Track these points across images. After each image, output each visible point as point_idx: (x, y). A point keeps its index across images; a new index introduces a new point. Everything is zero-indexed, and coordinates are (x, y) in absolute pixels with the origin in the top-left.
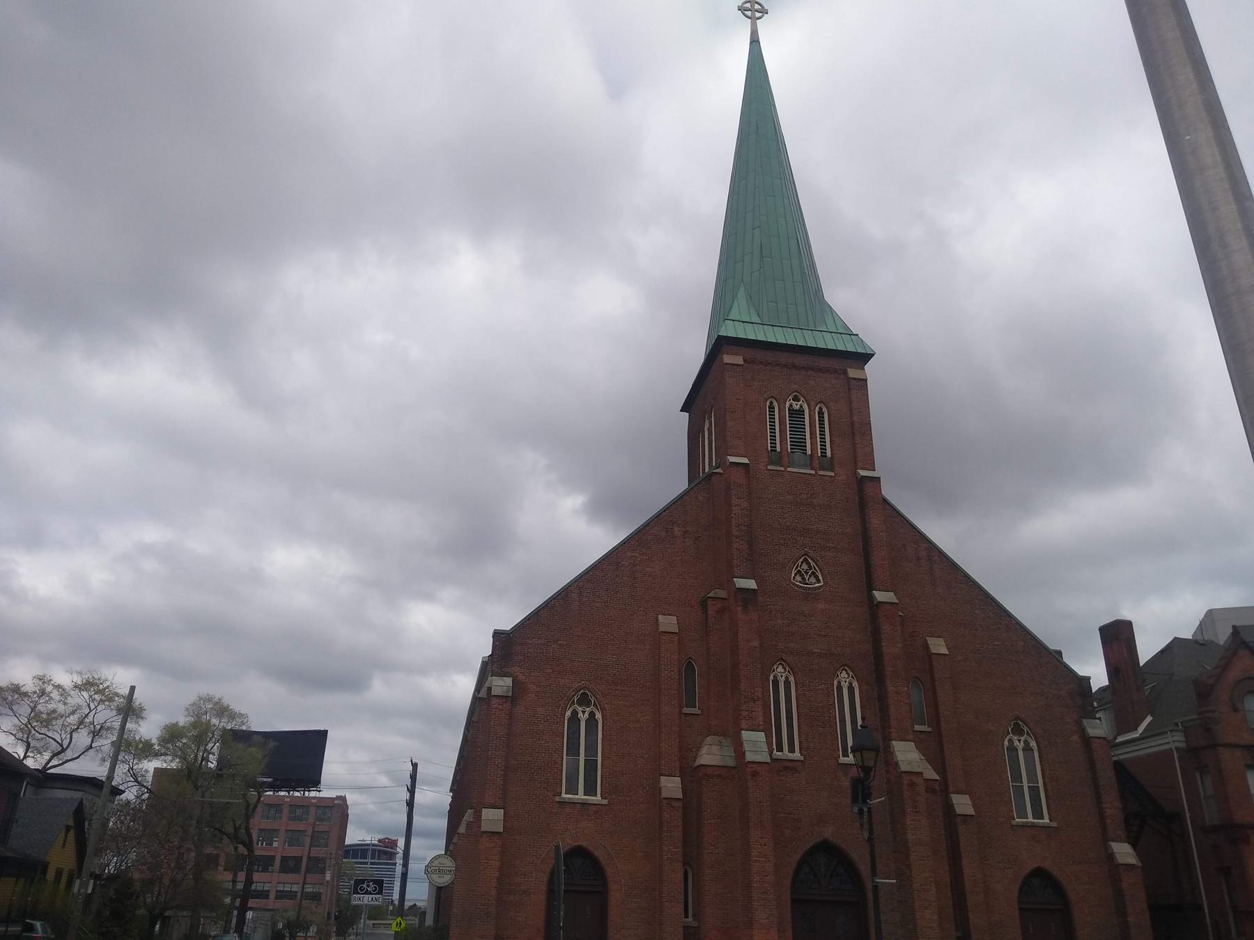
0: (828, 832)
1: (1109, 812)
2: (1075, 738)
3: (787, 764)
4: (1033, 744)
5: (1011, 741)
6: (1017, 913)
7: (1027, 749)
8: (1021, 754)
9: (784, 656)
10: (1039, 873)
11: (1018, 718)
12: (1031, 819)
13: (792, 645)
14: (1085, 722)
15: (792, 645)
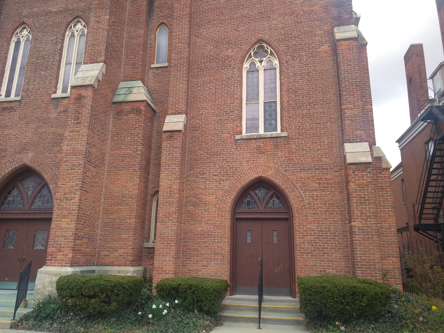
0: (27, 159)
1: (348, 113)
2: (325, 47)
3: (6, 105)
4: (276, 62)
5: (253, 64)
6: (228, 223)
7: (270, 69)
8: (261, 74)
9: (26, 20)
10: (260, 183)
11: (261, 41)
12: (261, 131)
13: (35, 10)
14: (336, 29)
15: (35, 10)
